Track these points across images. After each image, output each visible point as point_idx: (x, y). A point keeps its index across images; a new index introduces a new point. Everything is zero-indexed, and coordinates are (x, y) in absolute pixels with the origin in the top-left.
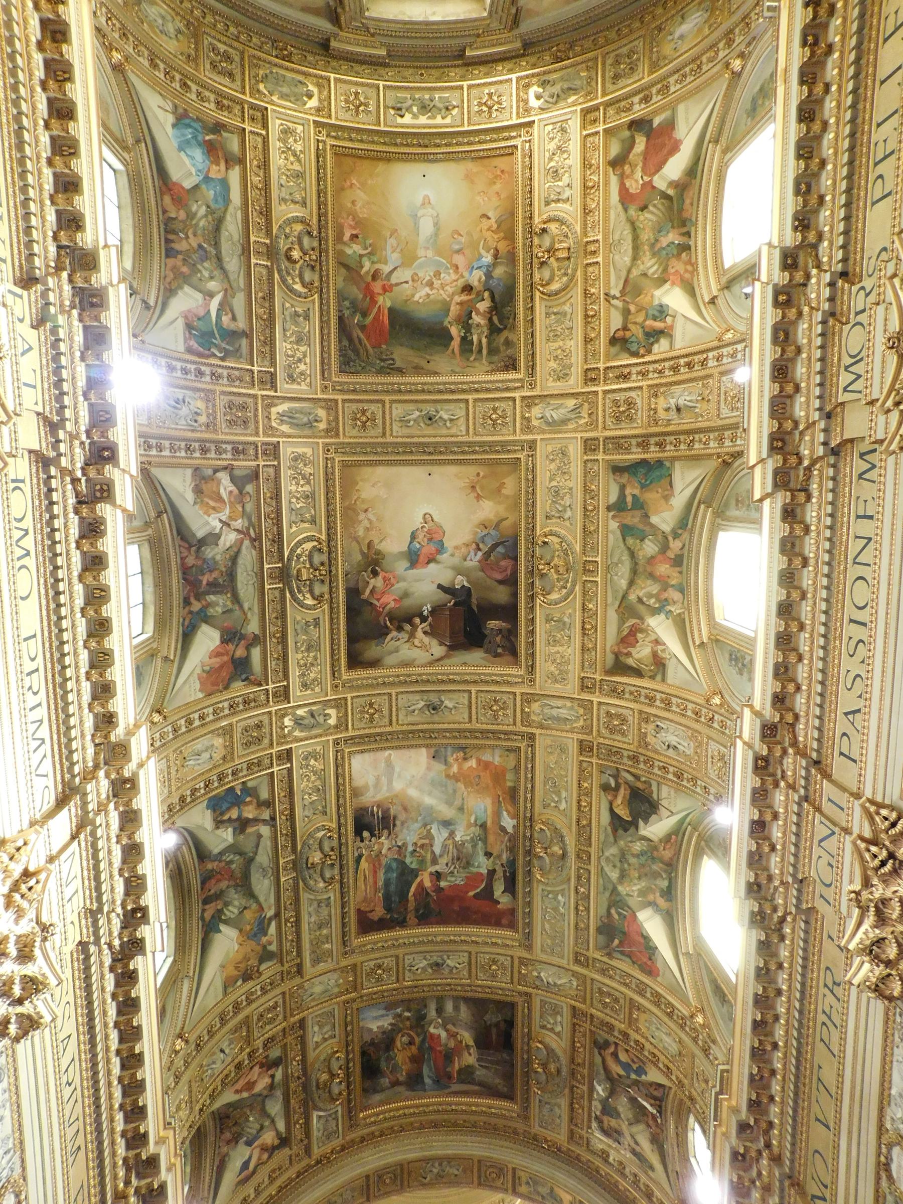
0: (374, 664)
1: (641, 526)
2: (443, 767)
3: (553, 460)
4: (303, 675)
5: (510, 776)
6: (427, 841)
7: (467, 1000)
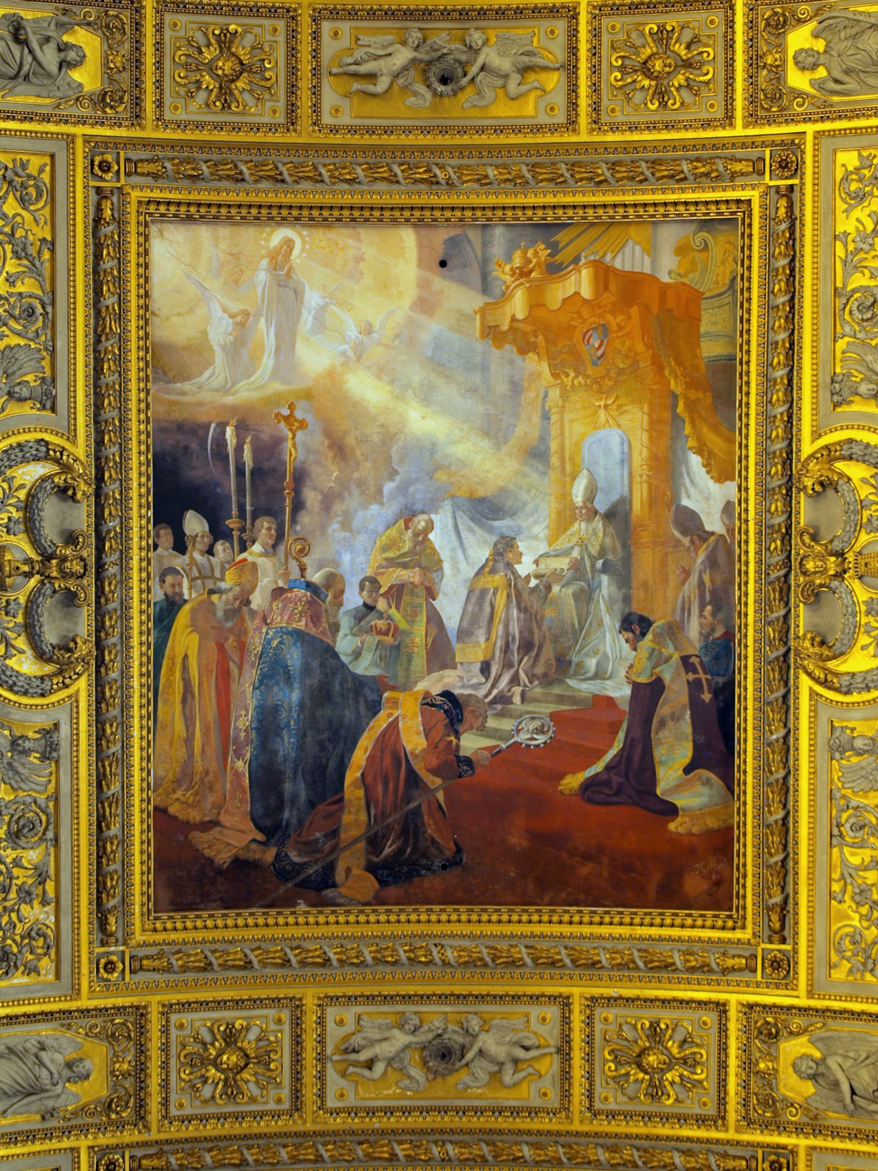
2: (477, 301)
6: (412, 576)
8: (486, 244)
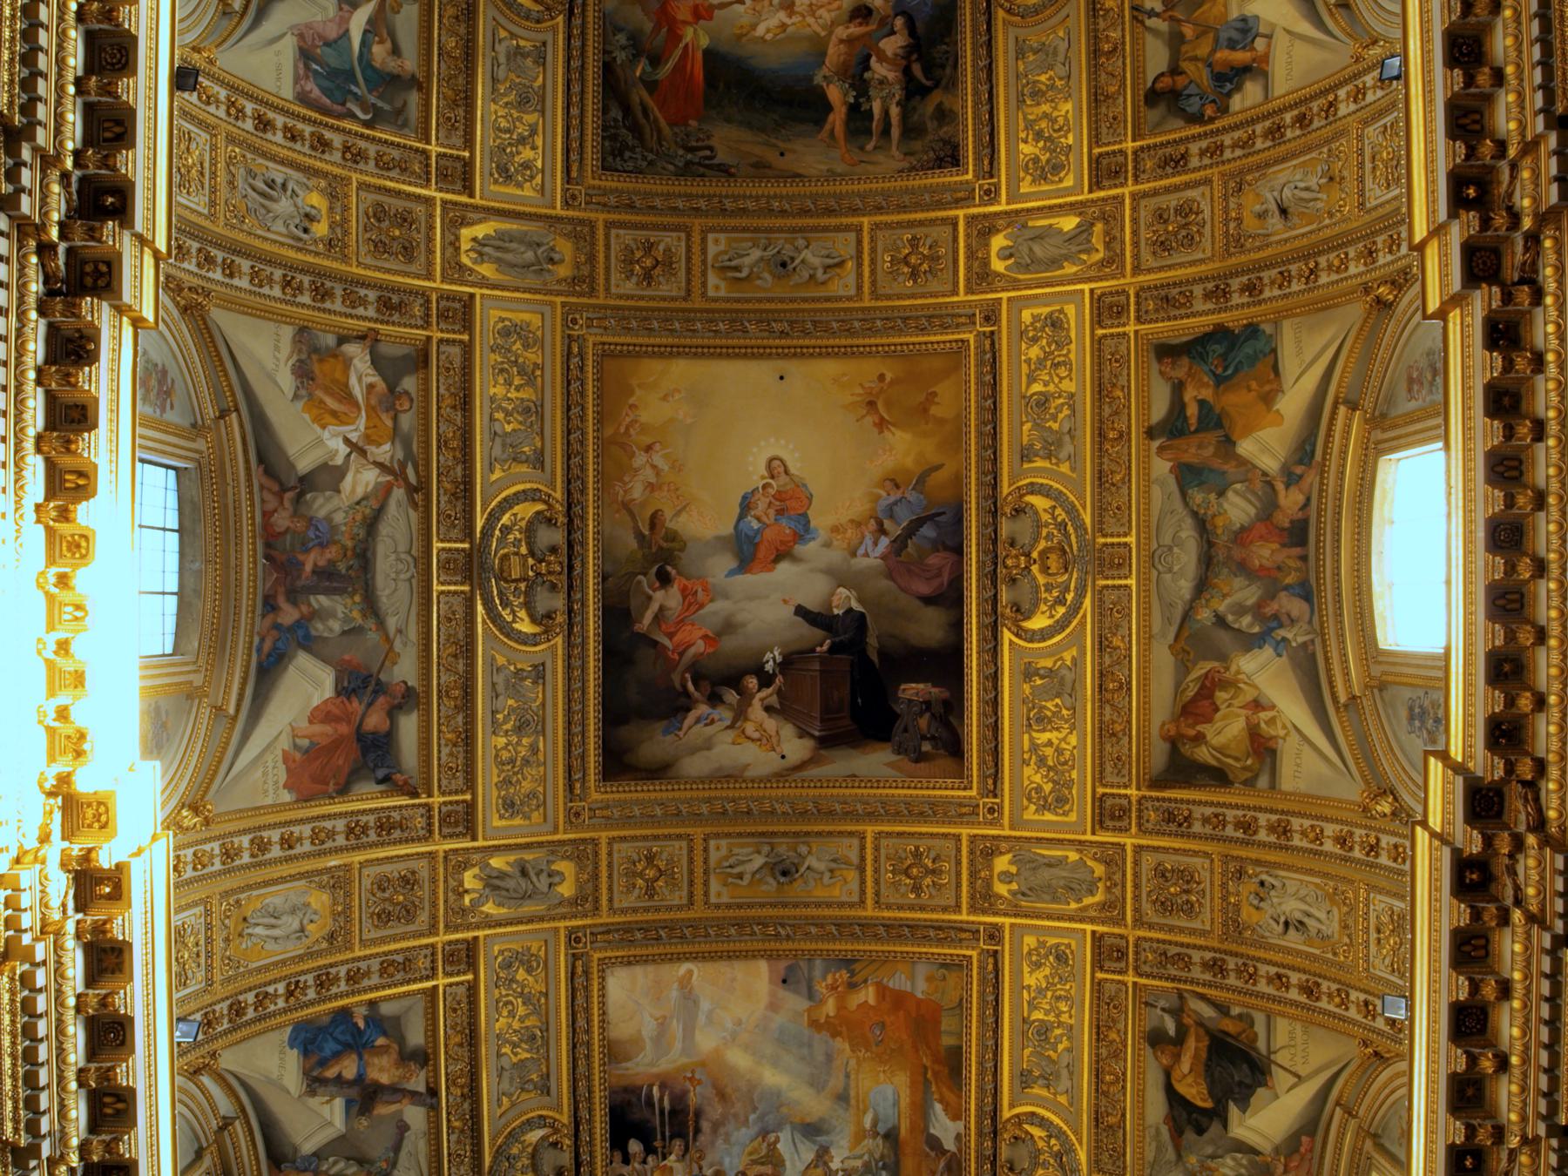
0: (659, 772)
1: (1217, 463)
3: (1035, 340)
4: (506, 782)
5: (947, 1023)
8: (811, 969)
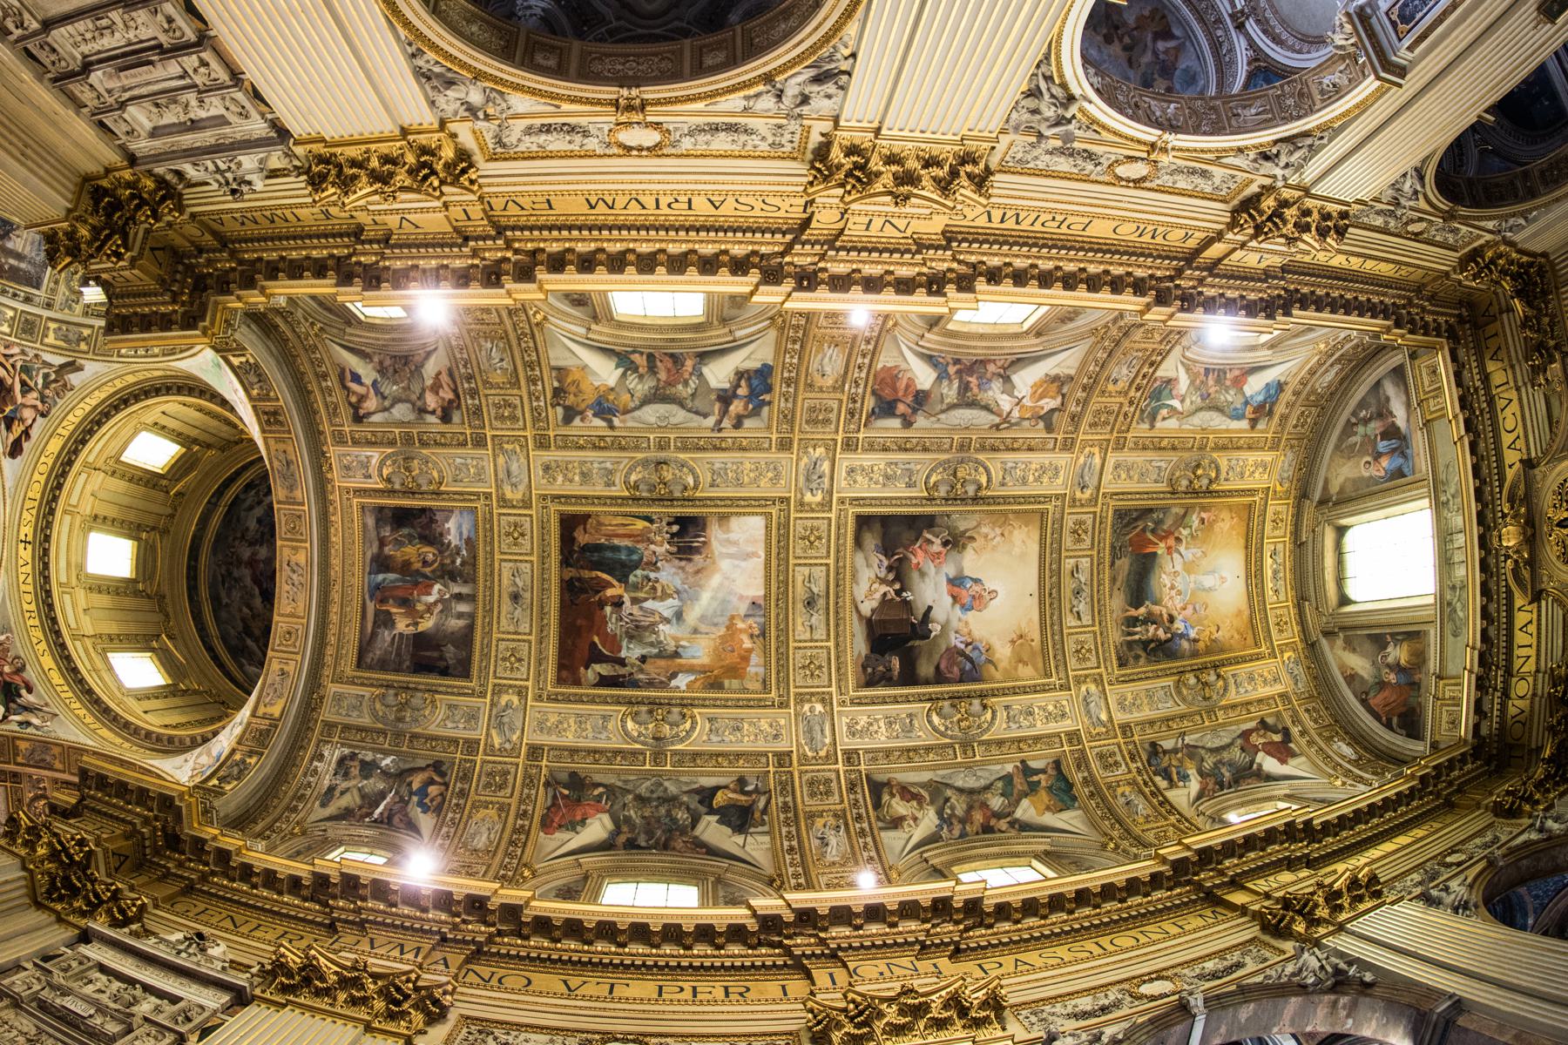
7: (471, 628)
